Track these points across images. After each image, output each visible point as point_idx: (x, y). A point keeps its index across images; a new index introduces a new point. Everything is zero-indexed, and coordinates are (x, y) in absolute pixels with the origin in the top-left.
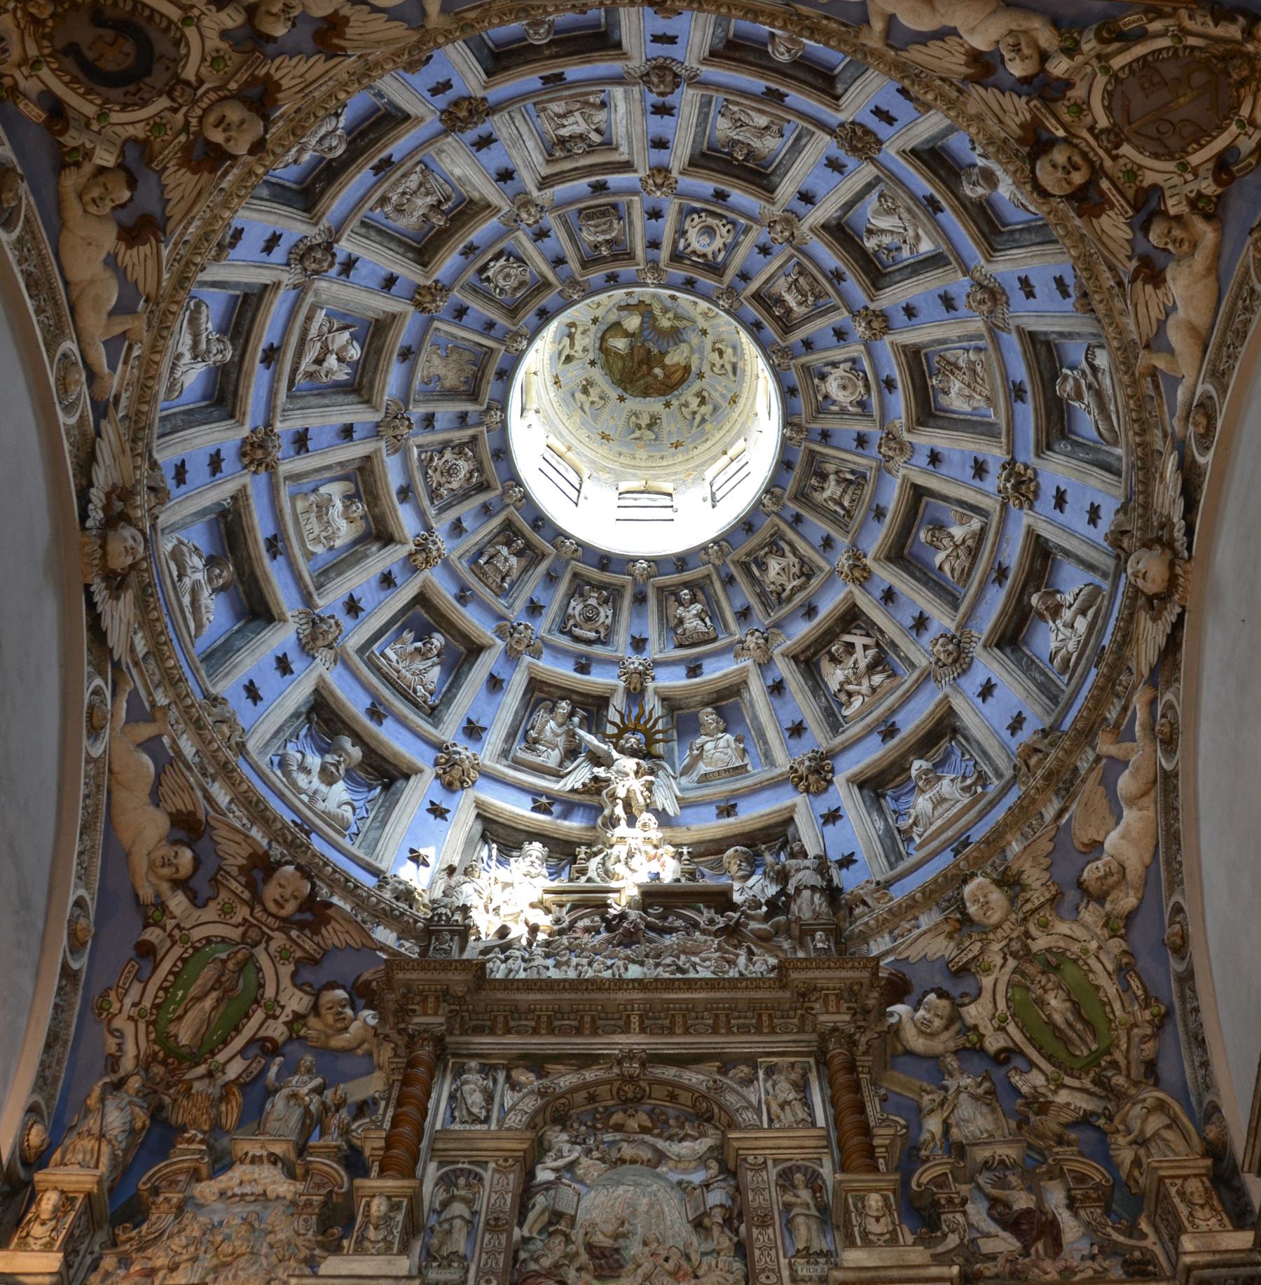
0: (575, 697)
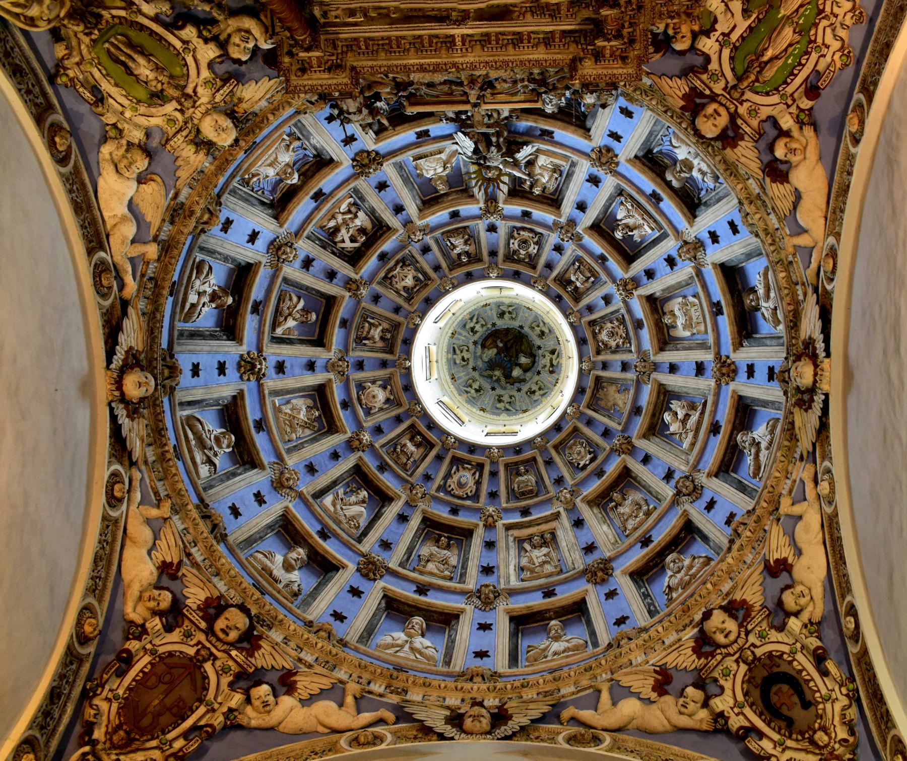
0: (531, 196)
